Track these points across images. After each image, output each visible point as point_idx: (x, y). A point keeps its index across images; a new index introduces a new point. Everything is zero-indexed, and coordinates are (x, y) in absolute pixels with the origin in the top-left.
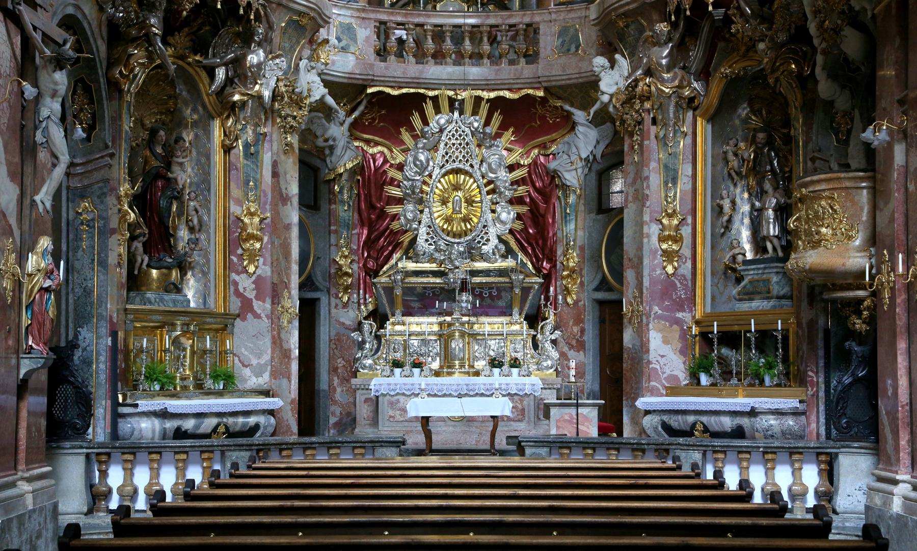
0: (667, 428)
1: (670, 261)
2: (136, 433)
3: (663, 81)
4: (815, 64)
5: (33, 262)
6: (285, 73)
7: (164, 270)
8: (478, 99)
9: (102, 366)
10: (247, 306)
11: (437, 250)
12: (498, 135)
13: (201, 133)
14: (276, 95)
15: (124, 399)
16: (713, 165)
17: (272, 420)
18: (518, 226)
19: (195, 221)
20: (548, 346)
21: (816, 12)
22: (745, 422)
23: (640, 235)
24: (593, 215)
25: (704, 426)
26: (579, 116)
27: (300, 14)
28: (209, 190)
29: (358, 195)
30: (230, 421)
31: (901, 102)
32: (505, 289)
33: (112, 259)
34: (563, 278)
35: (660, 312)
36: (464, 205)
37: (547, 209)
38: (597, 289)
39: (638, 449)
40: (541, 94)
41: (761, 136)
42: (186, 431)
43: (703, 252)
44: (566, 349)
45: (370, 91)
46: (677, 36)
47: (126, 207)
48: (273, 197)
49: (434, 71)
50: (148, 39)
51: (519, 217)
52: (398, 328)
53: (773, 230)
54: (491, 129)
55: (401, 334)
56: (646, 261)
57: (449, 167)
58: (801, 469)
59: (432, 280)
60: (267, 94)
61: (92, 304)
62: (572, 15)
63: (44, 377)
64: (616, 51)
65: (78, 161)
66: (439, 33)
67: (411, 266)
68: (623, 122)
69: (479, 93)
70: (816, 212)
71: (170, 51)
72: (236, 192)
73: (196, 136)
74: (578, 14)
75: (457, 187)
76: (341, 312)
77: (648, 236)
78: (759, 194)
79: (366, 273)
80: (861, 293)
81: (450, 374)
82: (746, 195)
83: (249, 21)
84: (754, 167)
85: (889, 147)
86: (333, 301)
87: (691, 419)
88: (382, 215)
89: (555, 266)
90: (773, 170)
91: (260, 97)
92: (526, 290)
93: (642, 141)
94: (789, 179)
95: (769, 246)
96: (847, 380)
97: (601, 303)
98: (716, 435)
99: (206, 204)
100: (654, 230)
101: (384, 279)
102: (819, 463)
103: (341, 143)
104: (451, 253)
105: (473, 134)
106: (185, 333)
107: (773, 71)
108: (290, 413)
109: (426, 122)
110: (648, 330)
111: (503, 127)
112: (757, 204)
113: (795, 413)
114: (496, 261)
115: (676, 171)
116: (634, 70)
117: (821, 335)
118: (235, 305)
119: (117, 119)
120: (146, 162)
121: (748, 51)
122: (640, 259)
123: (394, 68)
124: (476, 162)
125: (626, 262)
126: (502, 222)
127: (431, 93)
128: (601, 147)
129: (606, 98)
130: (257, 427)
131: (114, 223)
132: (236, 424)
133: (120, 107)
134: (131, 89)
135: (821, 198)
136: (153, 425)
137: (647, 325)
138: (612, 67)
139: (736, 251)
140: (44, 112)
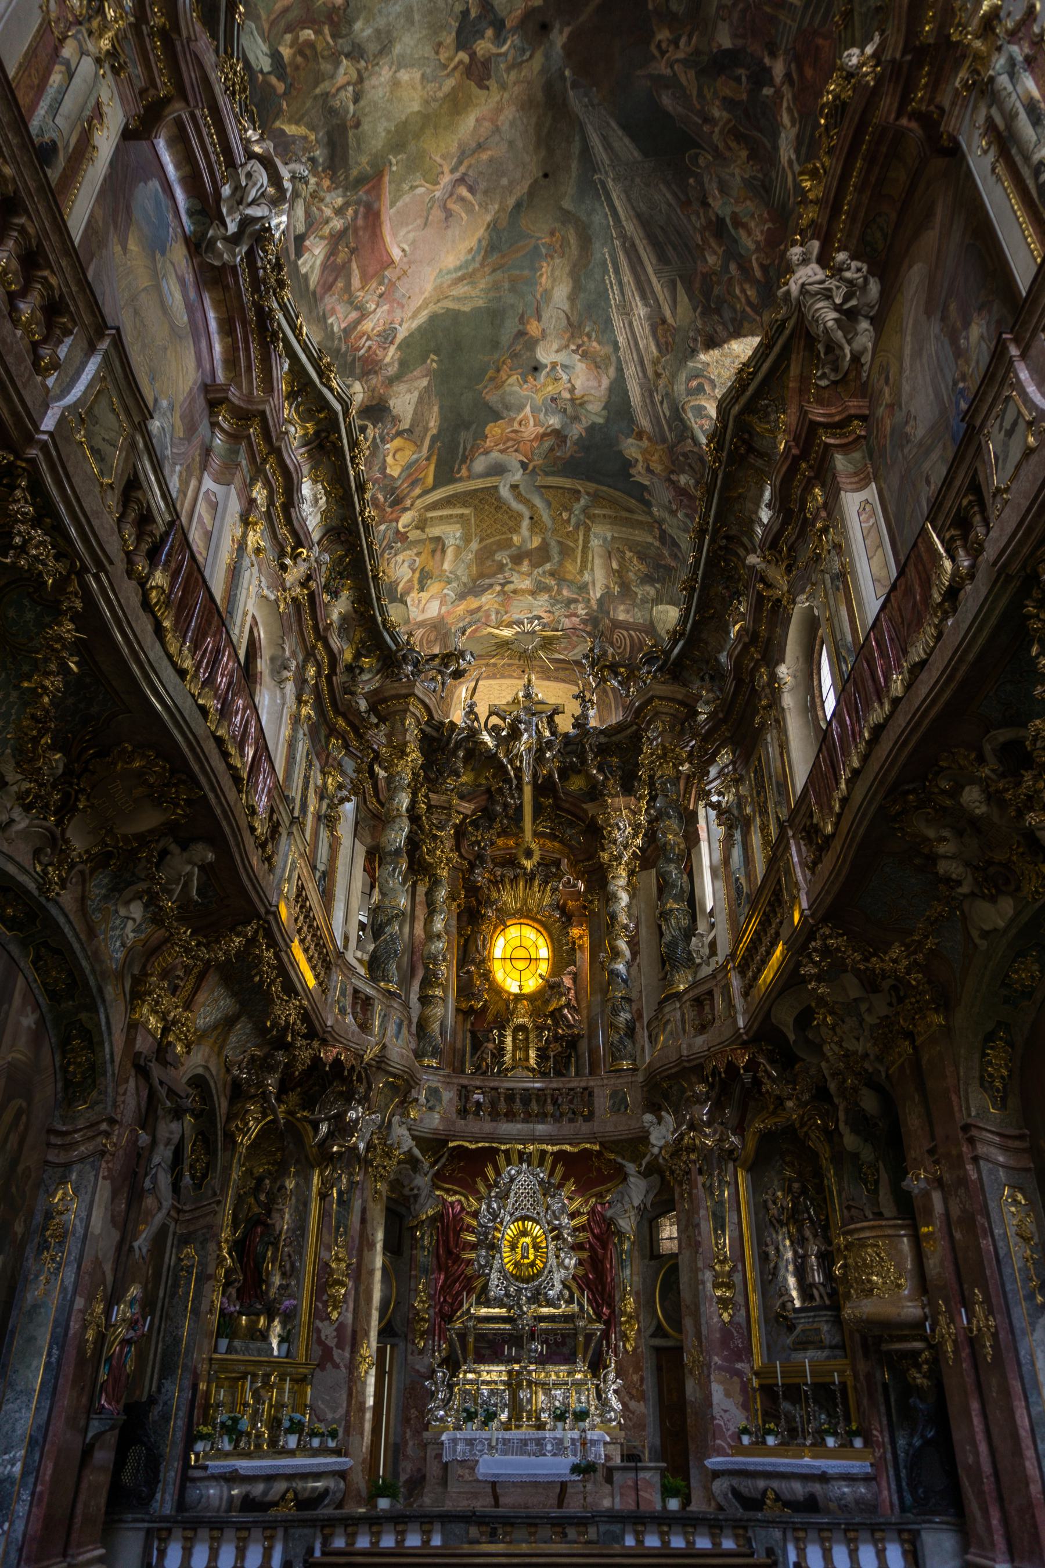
0: (736, 1493)
1: (726, 1309)
2: (203, 1500)
3: (706, 1136)
4: (837, 1120)
5: (121, 1311)
6: (379, 1128)
7: (253, 1317)
8: (544, 1153)
9: (180, 1423)
10: (327, 1355)
11: (507, 1295)
12: (561, 1186)
13: (302, 1182)
14: (370, 1147)
15: (196, 1461)
16: (756, 1214)
17: (342, 1485)
18: (581, 1272)
19: (288, 1266)
20: (611, 1395)
21: (833, 1075)
22: (817, 1488)
23: (696, 1283)
24: (646, 1261)
25: (776, 1494)
26: (631, 1168)
27: (394, 1076)
28: (303, 1235)
29: (438, 1241)
30: (299, 1485)
31: (931, 1152)
32: (568, 1335)
33: (204, 1307)
34: (621, 1323)
36: (531, 1251)
37: (606, 1253)
38: (653, 1336)
39: (714, 1526)
40: (597, 1148)
41: (796, 1185)
42: (254, 1499)
43: (754, 1298)
44: (627, 1399)
45: (451, 1145)
46: (713, 1094)
47: (225, 1253)
48: (361, 1243)
49: (507, 1128)
50: (265, 1096)
51: (580, 1263)
52: (470, 1376)
53: (818, 1278)
54: (555, 1181)
55: (471, 1382)
56: (702, 1309)
57: (517, 1214)
58: (884, 1550)
59: (502, 1326)
60: (362, 1146)
61: (179, 1353)
62: (620, 1081)
63: (112, 1438)
64: (660, 1109)
65: (187, 1208)
66: (510, 1096)
67: (484, 1311)
68: (672, 1172)
69: (544, 1147)
70: (865, 1260)
71: (283, 1108)
72: (326, 1237)
73: (297, 1185)
74: (625, 1080)
75: (524, 1233)
77: (703, 1283)
78: (798, 1241)
79: (442, 1319)
80: (918, 1345)
81: (518, 1427)
82: (788, 1243)
83: (352, 1081)
84: (793, 1216)
85: (926, 1195)
86: (410, 1346)
87: (761, 1484)
88: (457, 1259)
89: (613, 1312)
90: (810, 1218)
91: (355, 1147)
92: (589, 1337)
93: (691, 1189)
94: (826, 1228)
95: (815, 1292)
96: (917, 1442)
97: (658, 1350)
98: (787, 1504)
99: (300, 1250)
100: (708, 1275)
101: (458, 1325)
102: (902, 1542)
103: (424, 1193)
104: (519, 1299)
105: (540, 1183)
106: (266, 1383)
107: (802, 1125)
108: (360, 1474)
109: (498, 1173)
110: (710, 1382)
111: (565, 1178)
112: (800, 1251)
113: (867, 1479)
114: (560, 1307)
115: (723, 1218)
116: (679, 1125)
117: (880, 1389)
119: (227, 1169)
120: (250, 1209)
121: (776, 1108)
123: (473, 1126)
124: (541, 1210)
125: (683, 1309)
126: (567, 1268)
127: (503, 1147)
128: (651, 1196)
129: (656, 1150)
130: (326, 1491)
131: (210, 1270)
132: (305, 1489)
133: (232, 1156)
134: (244, 1141)
135: (867, 1246)
136: (222, 1492)
137: (709, 1376)
138: (659, 1123)
139: (785, 1298)
140: (156, 1159)
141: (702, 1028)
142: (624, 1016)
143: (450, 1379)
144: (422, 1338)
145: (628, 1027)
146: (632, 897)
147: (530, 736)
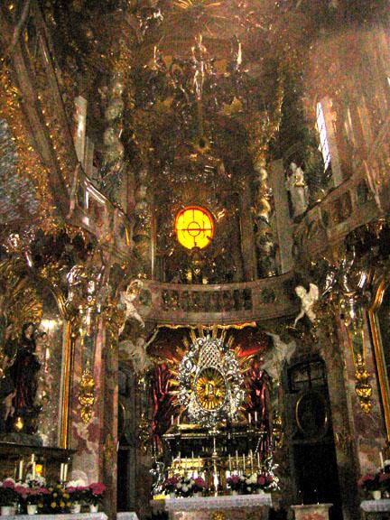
10: (82, 444)
26: (276, 338)
35: (363, 439)
38: (293, 438)
56: (350, 405)
62: (269, 283)
67: (183, 427)
72: (78, 367)
75: (210, 379)
76: (143, 458)
88: (168, 397)
97: (295, 446)
100: (352, 384)
109: (190, 341)
115: (361, 346)
118: (74, 444)
122: (344, 404)
123: (173, 313)
141: (341, 219)
142: (269, 244)
143: (166, 467)
144: (145, 445)
145: (272, 251)
146: (269, 174)
147: (200, 72)
